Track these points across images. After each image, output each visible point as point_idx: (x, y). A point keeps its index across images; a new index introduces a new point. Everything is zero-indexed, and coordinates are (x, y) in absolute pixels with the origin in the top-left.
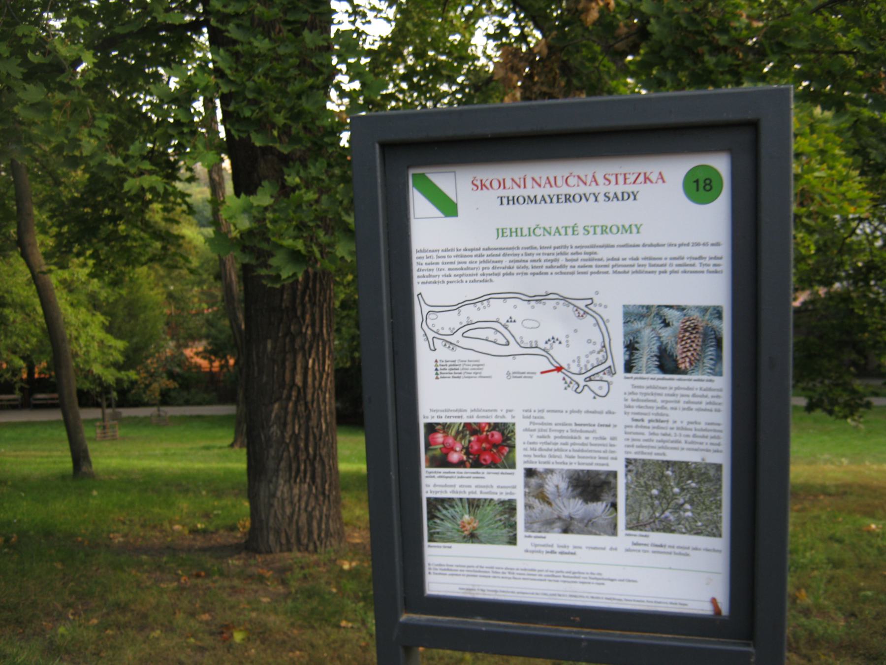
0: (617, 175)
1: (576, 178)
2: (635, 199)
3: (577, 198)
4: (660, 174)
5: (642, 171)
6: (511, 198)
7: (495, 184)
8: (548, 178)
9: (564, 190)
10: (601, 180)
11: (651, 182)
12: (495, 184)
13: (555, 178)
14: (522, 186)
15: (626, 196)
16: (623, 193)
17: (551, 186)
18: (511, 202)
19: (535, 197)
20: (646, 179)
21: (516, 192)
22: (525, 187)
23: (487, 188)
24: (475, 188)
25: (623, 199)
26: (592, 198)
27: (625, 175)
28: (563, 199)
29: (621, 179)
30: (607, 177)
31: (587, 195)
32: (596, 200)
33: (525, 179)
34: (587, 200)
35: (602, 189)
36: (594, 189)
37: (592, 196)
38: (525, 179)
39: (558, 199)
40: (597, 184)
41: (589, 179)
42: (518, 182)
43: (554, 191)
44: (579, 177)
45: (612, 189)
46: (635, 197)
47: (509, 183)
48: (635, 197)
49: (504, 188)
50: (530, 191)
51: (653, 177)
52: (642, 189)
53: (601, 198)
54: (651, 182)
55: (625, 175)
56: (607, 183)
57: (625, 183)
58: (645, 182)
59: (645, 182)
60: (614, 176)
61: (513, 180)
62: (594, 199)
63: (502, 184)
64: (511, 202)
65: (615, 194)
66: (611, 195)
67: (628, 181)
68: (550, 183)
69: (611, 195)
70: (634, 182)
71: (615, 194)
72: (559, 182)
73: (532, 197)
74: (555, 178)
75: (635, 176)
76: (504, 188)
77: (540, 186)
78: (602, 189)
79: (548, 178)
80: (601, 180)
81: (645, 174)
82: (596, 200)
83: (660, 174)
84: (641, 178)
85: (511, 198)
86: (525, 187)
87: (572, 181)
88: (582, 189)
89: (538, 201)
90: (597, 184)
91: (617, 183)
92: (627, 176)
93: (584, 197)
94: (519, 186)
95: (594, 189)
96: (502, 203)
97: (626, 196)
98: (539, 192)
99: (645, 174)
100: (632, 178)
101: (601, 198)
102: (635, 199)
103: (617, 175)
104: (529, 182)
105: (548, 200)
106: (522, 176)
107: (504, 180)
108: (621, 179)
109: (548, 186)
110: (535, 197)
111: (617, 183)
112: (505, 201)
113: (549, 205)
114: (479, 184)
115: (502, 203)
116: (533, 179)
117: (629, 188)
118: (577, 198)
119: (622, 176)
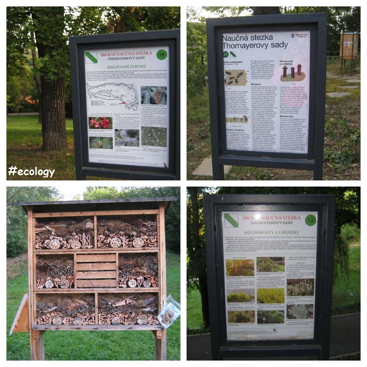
3: (275, 223)
5: (294, 215)
15: (289, 223)
26: (279, 223)
36: (280, 220)
52: (294, 221)
53: (282, 223)
66: (285, 222)
69: (285, 222)
72: (270, 218)
84: (294, 218)
95: (280, 220)
97: (289, 223)
100: (291, 218)
101: (282, 223)
114: (245, 217)
118: (275, 223)
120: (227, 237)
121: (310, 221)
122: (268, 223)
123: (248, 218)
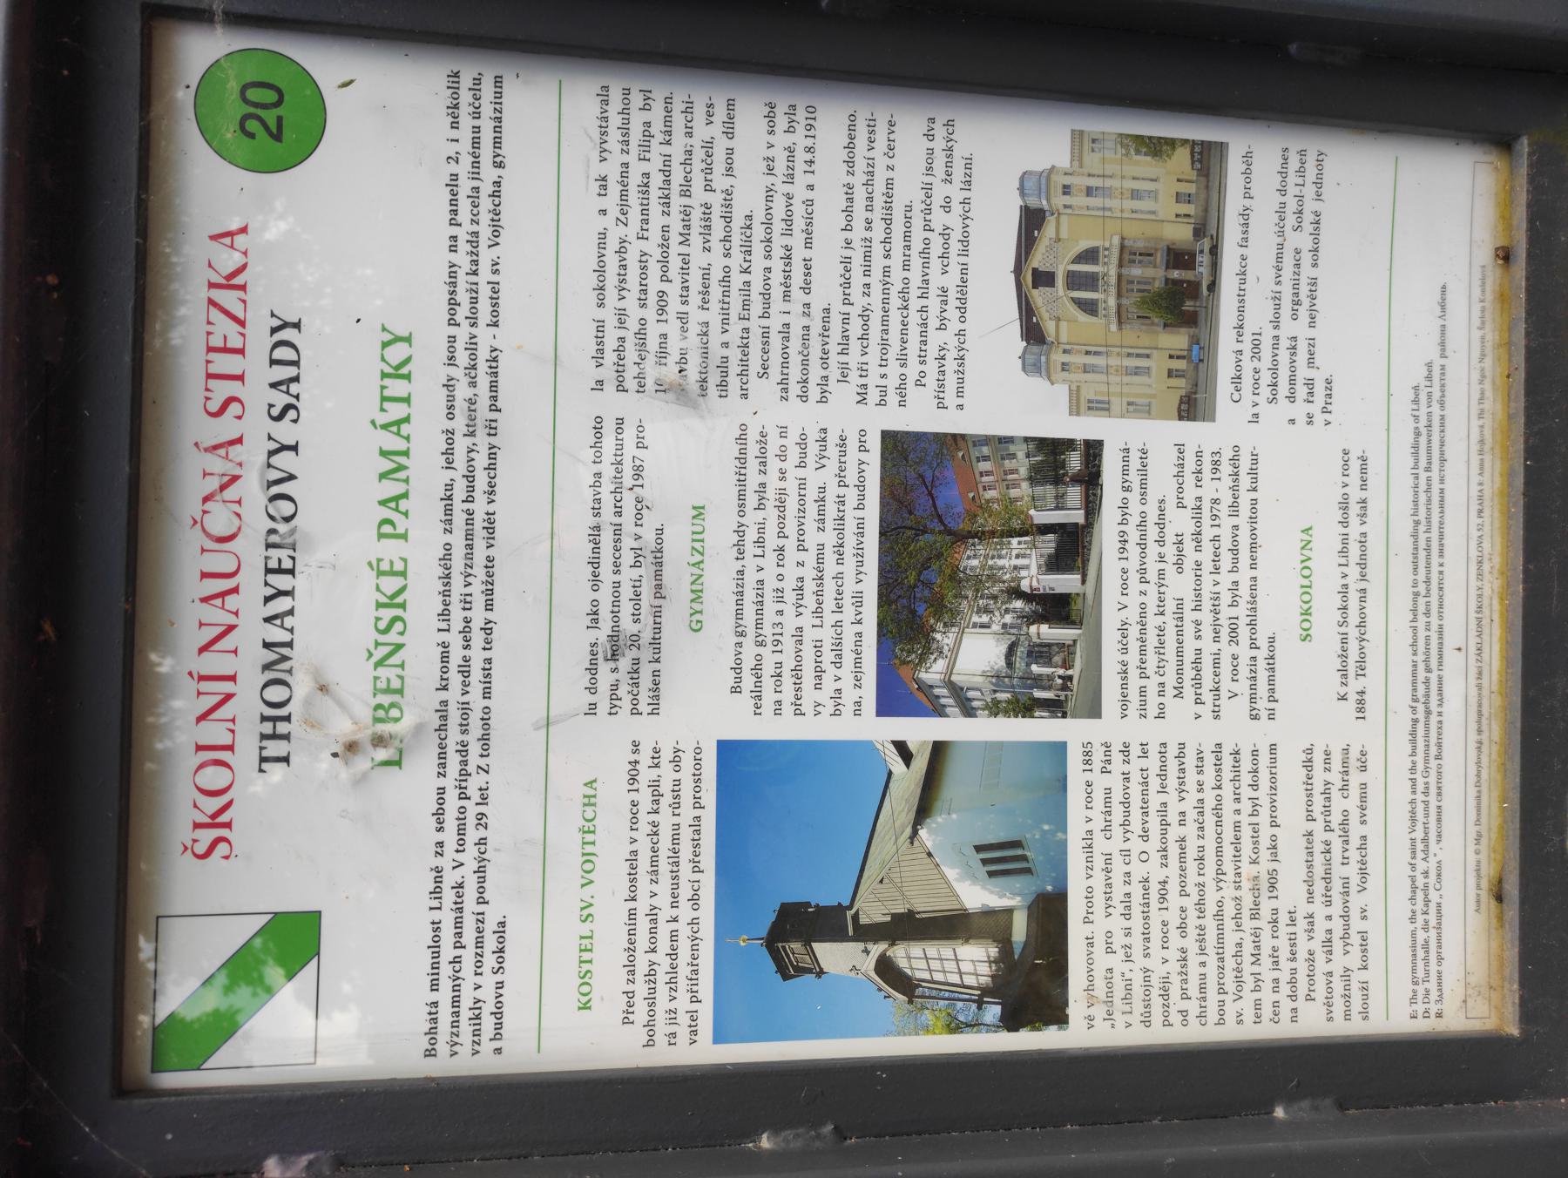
0: (210, 376)
1: (208, 506)
2: (297, 326)
4: (214, 238)
5: (204, 293)
6: (267, 728)
7: (214, 778)
8: (205, 600)
9: (250, 549)
10: (226, 428)
11: (244, 267)
12: (214, 778)
13: (204, 575)
14: (227, 687)
15: (283, 353)
16: (273, 362)
17: (235, 590)
18: (282, 728)
19: (267, 645)
20: (232, 281)
21: (247, 704)
22: (233, 678)
23: (230, 803)
24: (222, 848)
25: (296, 363)
26: (284, 460)
27: (210, 349)
28: (283, 554)
29: (224, 364)
30: (214, 406)
31: (274, 475)
32: (294, 448)
33: (202, 678)
34: (291, 477)
35: (257, 429)
36: (253, 454)
37: (276, 460)
38: (202, 678)
39: (280, 571)
40: (239, 441)
41: (216, 464)
42: (213, 700)
43: (252, 583)
44: (206, 499)
45: (258, 394)
46: (285, 325)
47: (214, 733)
48: (285, 325)
49: (230, 748)
50: (248, 662)
51: (228, 260)
53: (285, 432)
54: (244, 267)
55: (210, 349)
56: (234, 408)
57: (241, 351)
58: (243, 288)
59: (243, 288)
60: (212, 383)
61: (203, 717)
62: (287, 455)
63: (217, 754)
64: (282, 728)
65: (274, 385)
67: (234, 342)
68: (223, 595)
69: (281, 400)
70: (242, 323)
71: (274, 385)
72: (225, 564)
73: (271, 656)
74: (204, 575)
75: (215, 315)
76: (230, 748)
77: (231, 628)
78: (257, 429)
79: (205, 600)
80: (226, 428)
81: (212, 285)
82: (294, 448)
83: (214, 238)
84: (228, 299)
85: (267, 728)
86: (233, 678)
87: (220, 521)
88: (251, 489)
89: (286, 637)
90: (239, 441)
91: (240, 378)
92: (217, 341)
93: (279, 489)
94: (229, 697)
95: (253, 454)
96: (286, 760)
97: (283, 353)
98: (251, 634)
99: (212, 285)
101: (285, 432)
102: (297, 326)
103: (210, 376)
104: (214, 663)
105: (282, 604)
106: (193, 685)
107: (199, 748)
108: (224, 364)
109: (231, 601)
110: (267, 645)
111: (240, 378)
112: (275, 748)
113: (300, 602)
114: (208, 836)
115: (286, 760)
116: (202, 650)
117: (259, 340)
119: (212, 356)
120: (424, 1043)
121: (278, 129)
122: (282, 582)
123: (215, 804)
